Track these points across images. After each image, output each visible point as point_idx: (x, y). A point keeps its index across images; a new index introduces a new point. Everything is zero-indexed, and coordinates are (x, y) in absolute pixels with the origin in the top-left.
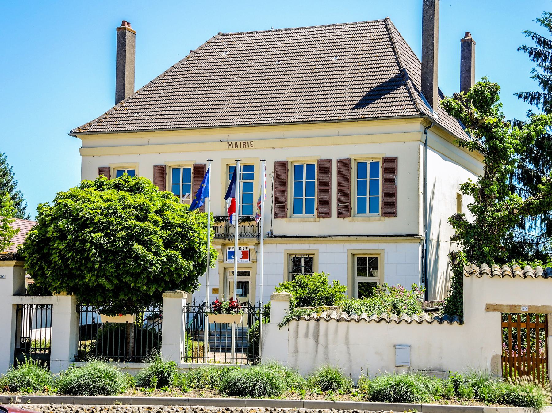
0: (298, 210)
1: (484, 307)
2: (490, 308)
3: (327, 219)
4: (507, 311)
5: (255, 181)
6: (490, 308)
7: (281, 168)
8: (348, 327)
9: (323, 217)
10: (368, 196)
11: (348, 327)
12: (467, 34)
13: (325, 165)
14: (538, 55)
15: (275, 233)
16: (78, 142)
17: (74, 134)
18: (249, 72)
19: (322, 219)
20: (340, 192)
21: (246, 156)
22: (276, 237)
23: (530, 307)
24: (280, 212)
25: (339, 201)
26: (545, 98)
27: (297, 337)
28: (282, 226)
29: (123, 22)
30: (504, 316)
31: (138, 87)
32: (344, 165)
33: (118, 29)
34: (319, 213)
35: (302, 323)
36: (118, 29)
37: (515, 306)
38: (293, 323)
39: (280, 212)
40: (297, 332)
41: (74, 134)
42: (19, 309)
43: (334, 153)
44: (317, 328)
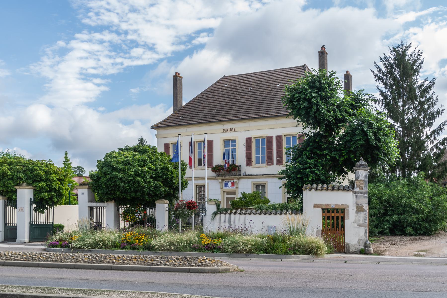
0: (257, 162)
1: (313, 206)
2: (316, 206)
3: (271, 166)
4: (324, 207)
5: (237, 148)
6: (316, 206)
7: (249, 141)
8: (245, 217)
9: (270, 165)
10: (260, 147)
11: (245, 217)
12: (347, 72)
13: (270, 139)
14: (379, 78)
15: (247, 174)
16: (155, 131)
17: (153, 127)
18: (236, 94)
19: (269, 166)
20: (277, 152)
21: (229, 136)
22: (247, 175)
23: (336, 205)
24: (249, 163)
25: (277, 157)
26: (382, 101)
27: (220, 222)
28: (250, 170)
29: (176, 73)
30: (323, 209)
31: (184, 104)
32: (279, 138)
33: (174, 76)
34: (268, 163)
35: (222, 215)
36: (174, 76)
37: (328, 205)
38: (218, 216)
39: (249, 163)
40: (220, 220)
41: (153, 127)
42: (91, 209)
43: (274, 133)
44: (230, 218)
